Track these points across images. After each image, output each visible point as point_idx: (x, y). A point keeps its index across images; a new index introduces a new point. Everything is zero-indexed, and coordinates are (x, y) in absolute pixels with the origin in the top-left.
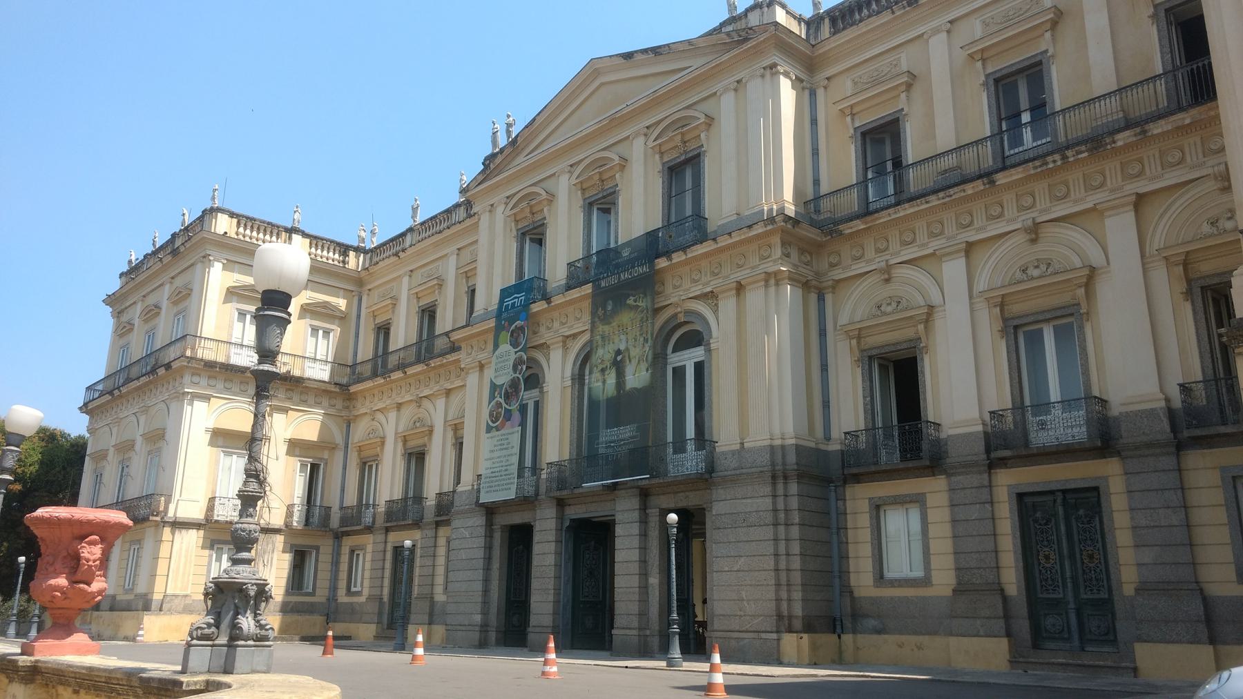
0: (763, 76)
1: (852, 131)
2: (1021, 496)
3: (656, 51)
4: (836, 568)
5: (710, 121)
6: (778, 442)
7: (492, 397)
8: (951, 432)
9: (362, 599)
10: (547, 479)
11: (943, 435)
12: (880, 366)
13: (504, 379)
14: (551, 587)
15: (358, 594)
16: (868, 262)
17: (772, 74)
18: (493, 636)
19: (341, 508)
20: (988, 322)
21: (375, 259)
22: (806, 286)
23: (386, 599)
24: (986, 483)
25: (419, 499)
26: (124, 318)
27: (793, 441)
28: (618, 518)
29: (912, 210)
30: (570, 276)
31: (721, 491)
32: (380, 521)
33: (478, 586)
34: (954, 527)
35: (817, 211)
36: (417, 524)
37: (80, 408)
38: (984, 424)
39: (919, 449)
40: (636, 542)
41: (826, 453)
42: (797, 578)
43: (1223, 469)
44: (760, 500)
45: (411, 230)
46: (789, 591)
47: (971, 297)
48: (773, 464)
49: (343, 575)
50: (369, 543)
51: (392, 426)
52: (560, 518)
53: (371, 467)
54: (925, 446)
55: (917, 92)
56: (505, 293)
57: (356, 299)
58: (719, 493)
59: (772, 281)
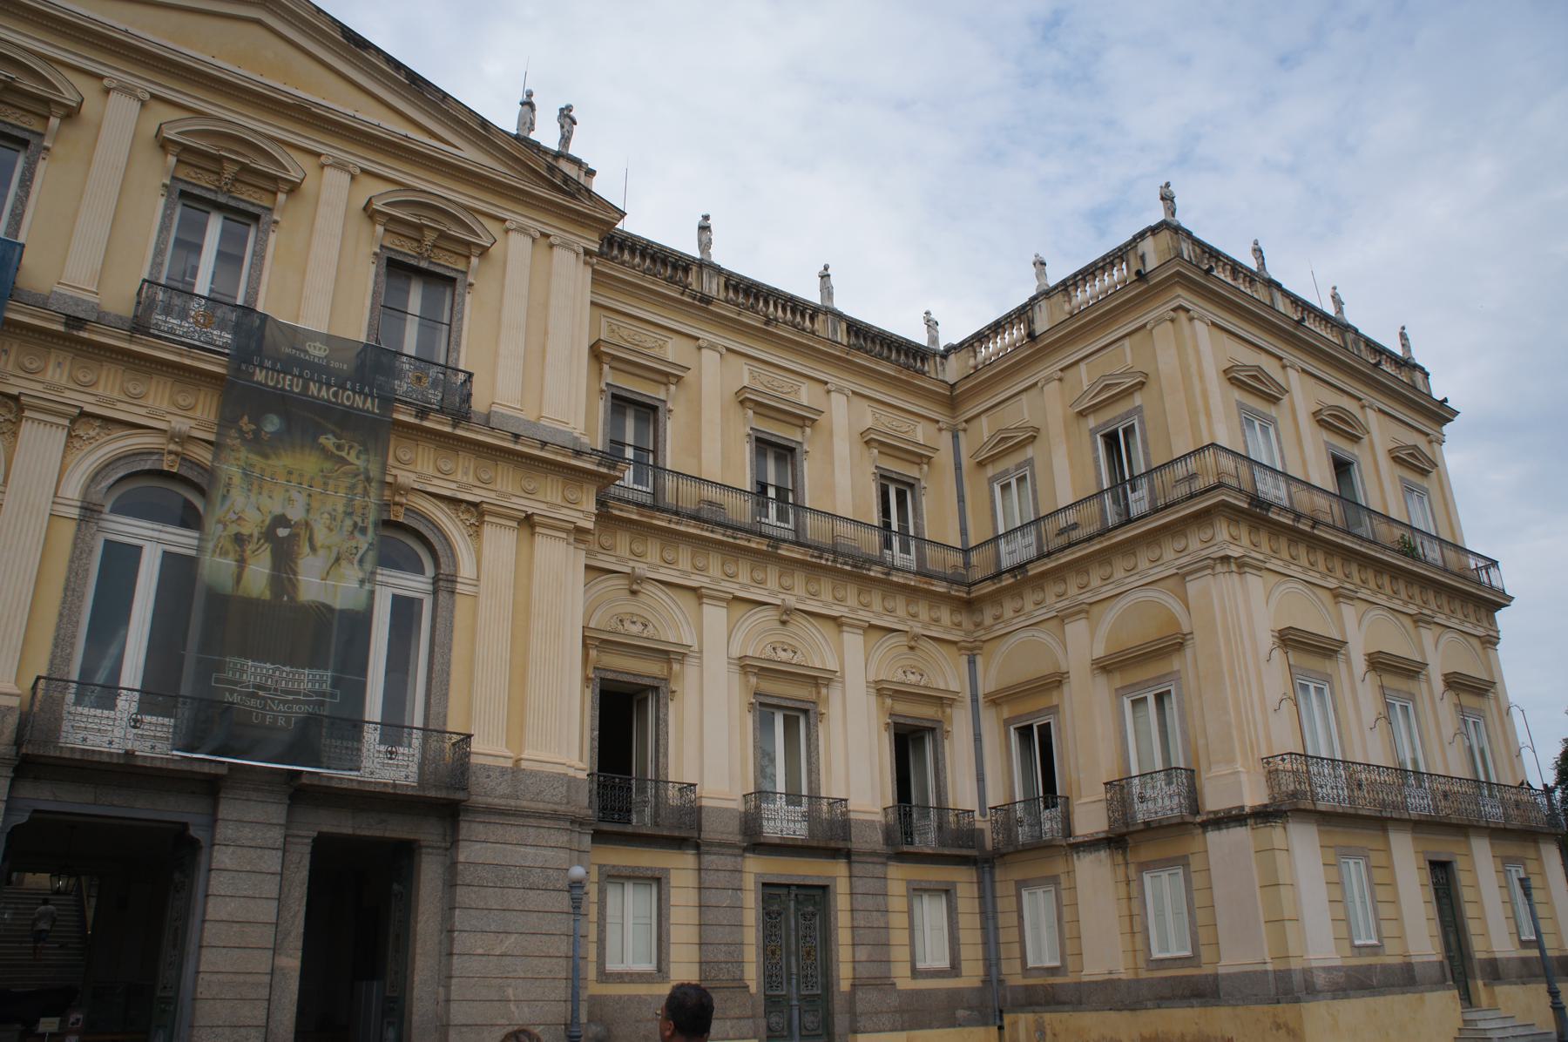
3: (416, 85)
43: (909, 882)
44: (549, 853)
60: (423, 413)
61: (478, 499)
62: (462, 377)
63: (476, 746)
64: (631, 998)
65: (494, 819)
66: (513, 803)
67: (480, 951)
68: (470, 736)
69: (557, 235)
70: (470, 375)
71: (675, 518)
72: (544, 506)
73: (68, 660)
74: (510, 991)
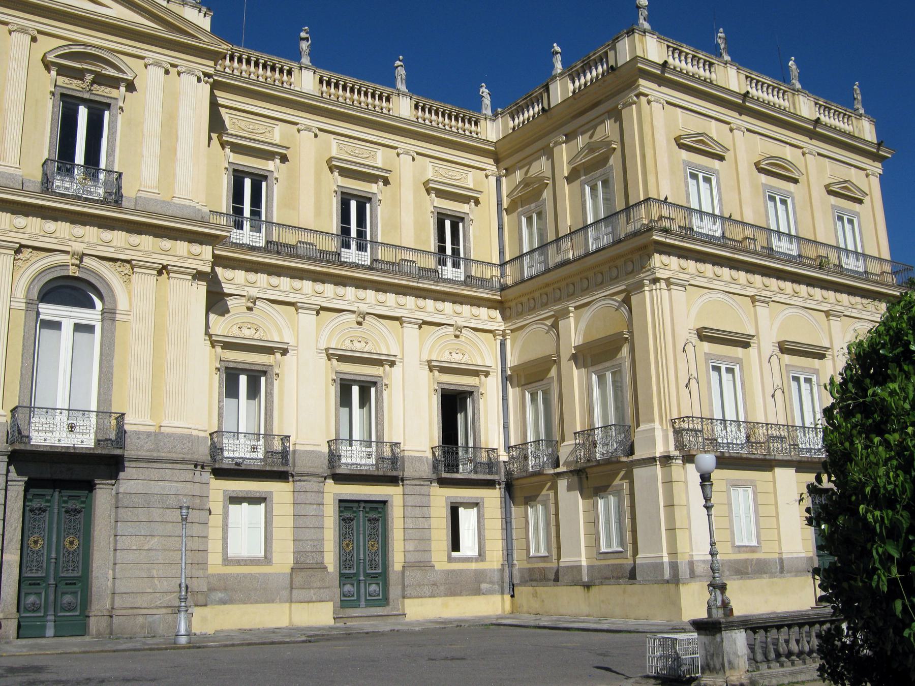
2: (340, 501)
44: (179, 485)
61: (129, 258)
62: (115, 176)
63: (127, 419)
64: (245, 576)
67: (134, 548)
68: (123, 414)
69: (183, 65)
70: (120, 174)
72: (175, 259)
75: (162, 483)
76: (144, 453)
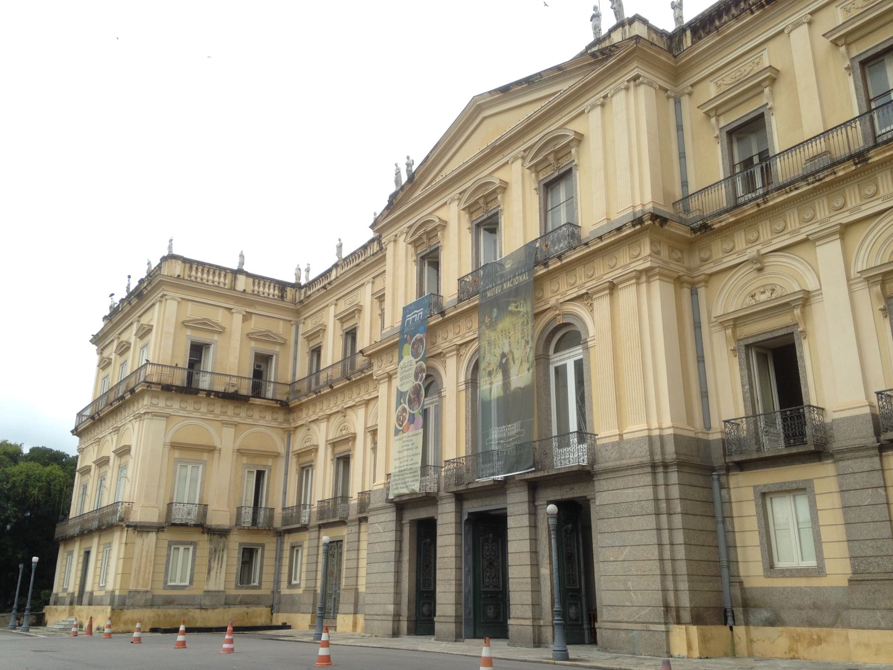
0: (627, 89)
1: (717, 132)
3: (531, 82)
4: (724, 559)
5: (579, 139)
6: (656, 433)
7: (398, 403)
8: (837, 416)
9: (300, 591)
10: (446, 477)
11: (828, 420)
12: (758, 355)
13: (407, 387)
14: (453, 577)
15: (297, 586)
16: (740, 253)
17: (636, 86)
18: (404, 625)
19: (284, 509)
20: (868, 301)
21: (309, 293)
22: (678, 281)
23: (319, 591)
24: (878, 466)
25: (345, 498)
26: (106, 354)
27: (671, 431)
28: (510, 511)
29: (782, 198)
30: (461, 291)
31: (604, 482)
32: (315, 522)
33: (391, 577)
34: (845, 514)
35: (687, 211)
36: (343, 523)
37: (72, 432)
38: (871, 406)
39: (803, 434)
40: (526, 533)
41: (707, 443)
42: (682, 568)
45: (336, 266)
46: (675, 582)
47: (848, 279)
48: (652, 454)
49: (285, 570)
50: (306, 540)
51: (322, 435)
52: (459, 511)
53: (307, 471)
54: (808, 431)
55: (781, 87)
56: (407, 310)
57: (294, 327)
58: (600, 484)
59: (644, 279)
60: (546, 265)
64: (794, 590)
65: (610, 475)
66: (618, 463)
67: (612, 559)
71: (760, 201)
73: (476, 448)
74: (630, 583)
75: (626, 491)
76: (610, 464)
